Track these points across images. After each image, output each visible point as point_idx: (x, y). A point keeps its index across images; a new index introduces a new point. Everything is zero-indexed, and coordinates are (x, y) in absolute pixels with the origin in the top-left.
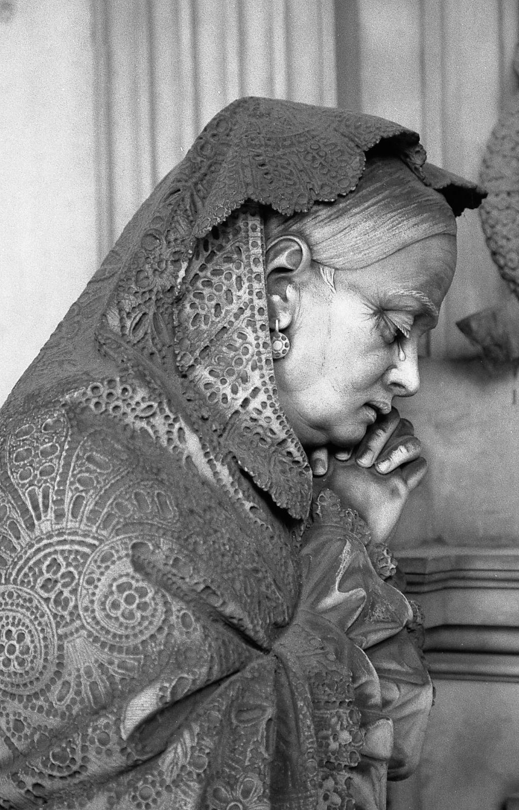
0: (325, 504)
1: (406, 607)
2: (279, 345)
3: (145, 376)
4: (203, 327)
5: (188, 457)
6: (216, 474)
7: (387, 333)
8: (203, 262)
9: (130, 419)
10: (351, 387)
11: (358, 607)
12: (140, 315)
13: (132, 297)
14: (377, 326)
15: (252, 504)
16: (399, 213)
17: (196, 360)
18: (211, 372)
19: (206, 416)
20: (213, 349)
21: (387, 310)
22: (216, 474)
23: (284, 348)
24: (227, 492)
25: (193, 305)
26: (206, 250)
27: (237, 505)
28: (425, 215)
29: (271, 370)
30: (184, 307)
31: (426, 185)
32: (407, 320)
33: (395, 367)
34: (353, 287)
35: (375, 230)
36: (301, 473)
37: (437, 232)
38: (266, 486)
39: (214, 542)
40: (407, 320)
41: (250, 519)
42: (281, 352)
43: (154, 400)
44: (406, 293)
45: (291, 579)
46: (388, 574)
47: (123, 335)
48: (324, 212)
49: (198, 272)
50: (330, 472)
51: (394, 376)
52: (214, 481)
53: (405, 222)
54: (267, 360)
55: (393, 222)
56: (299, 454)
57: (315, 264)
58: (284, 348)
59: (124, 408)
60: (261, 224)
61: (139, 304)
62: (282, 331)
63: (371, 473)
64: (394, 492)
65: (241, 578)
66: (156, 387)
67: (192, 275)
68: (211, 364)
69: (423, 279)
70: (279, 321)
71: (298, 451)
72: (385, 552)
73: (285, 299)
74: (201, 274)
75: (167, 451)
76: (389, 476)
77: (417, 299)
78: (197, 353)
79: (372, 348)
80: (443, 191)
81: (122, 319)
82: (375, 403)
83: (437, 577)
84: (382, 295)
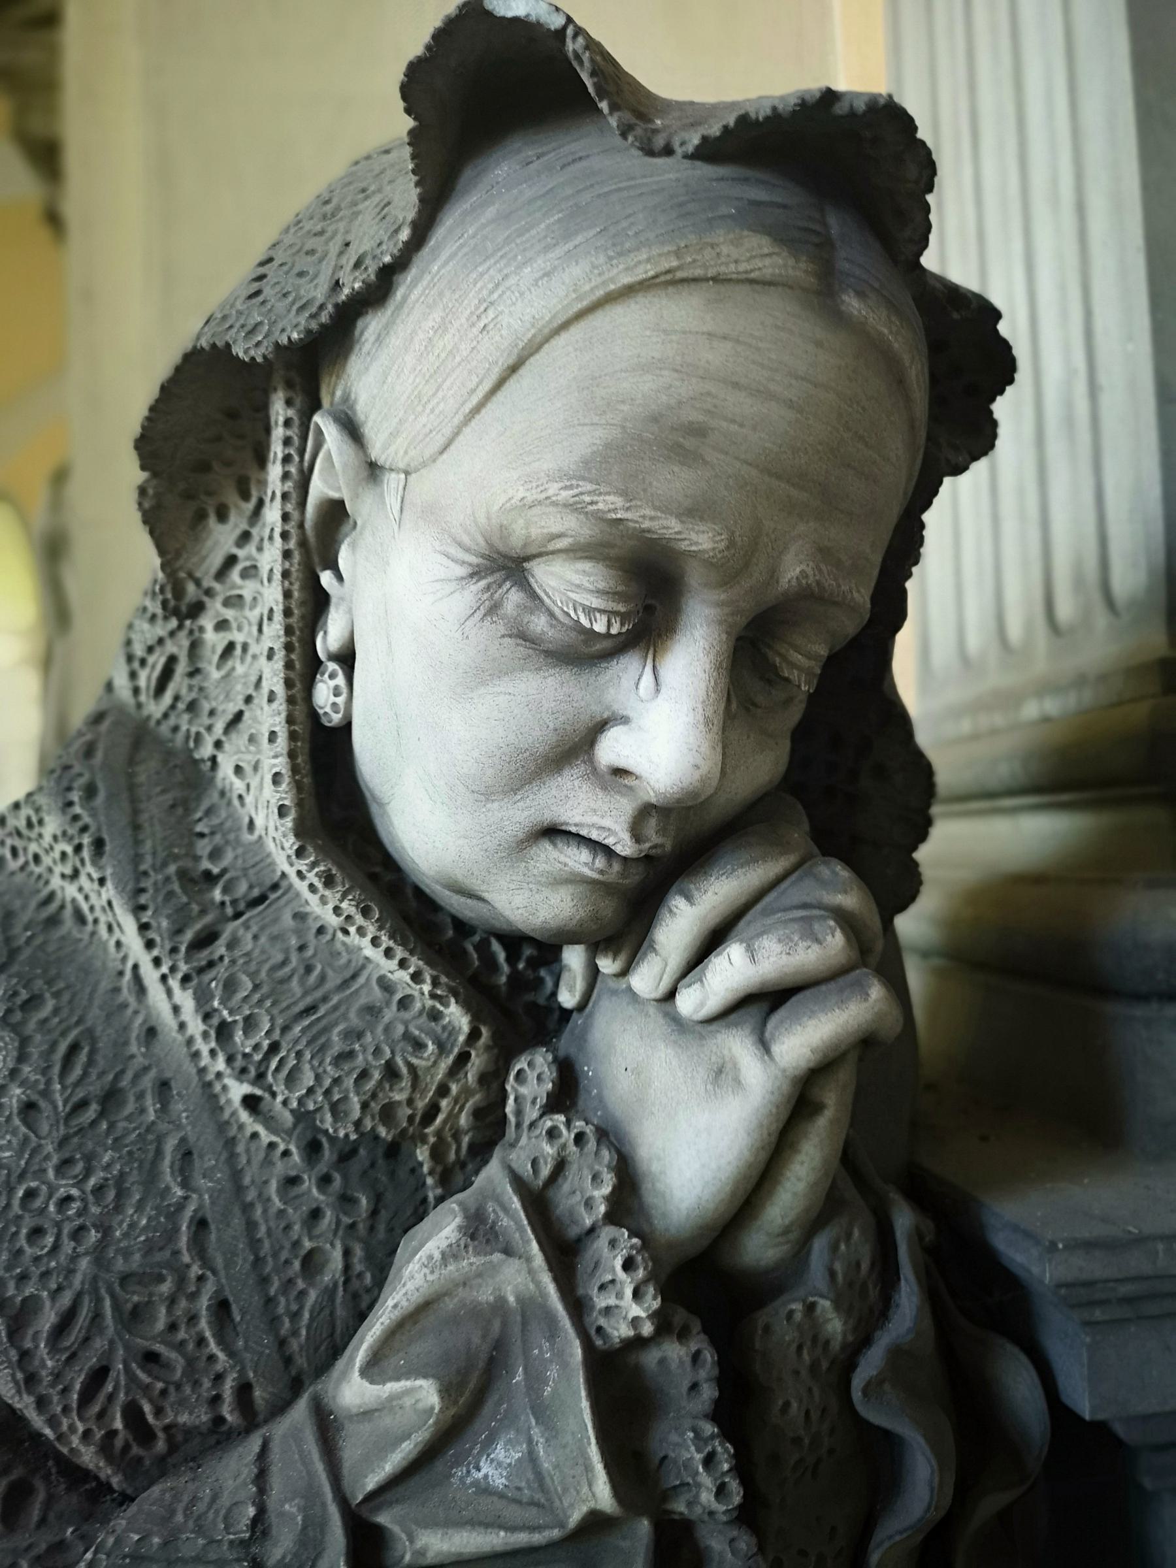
0: (523, 1090)
1: (588, 1468)
2: (324, 694)
3: (69, 789)
4: (240, 669)
5: (136, 967)
6: (176, 1009)
7: (539, 624)
8: (244, 526)
9: (56, 882)
10: (461, 788)
11: (407, 1436)
12: (162, 660)
13: (146, 626)
14: (494, 609)
15: (246, 1089)
16: (502, 257)
17: (218, 744)
18: (238, 770)
19: (216, 870)
20: (247, 715)
21: (528, 559)
22: (176, 1009)
23: (332, 699)
24: (196, 1055)
25: (222, 625)
26: (246, 496)
27: (217, 1088)
28: (579, 239)
29: (276, 757)
30: (201, 629)
31: (650, 152)
32: (576, 579)
33: (625, 720)
34: (431, 513)
35: (442, 328)
36: (435, 1016)
37: (627, 280)
38: (256, 1047)
39: (30, 1194)
40: (576, 579)
41: (241, 1127)
42: (328, 709)
43: (71, 839)
44: (531, 496)
45: (313, 1295)
46: (621, 1331)
47: (139, 706)
48: (371, 326)
49: (235, 551)
50: (590, 1004)
51: (613, 748)
52: (175, 1026)
53: (512, 281)
54: (272, 737)
55: (481, 289)
56: (393, 964)
57: (373, 470)
58: (332, 699)
59: (47, 860)
60: (289, 403)
61: (161, 641)
62: (334, 657)
63: (666, 1015)
64: (722, 1074)
65: (66, 1299)
66: (77, 809)
67: (217, 560)
68: (239, 752)
69: (589, 440)
70: (325, 633)
71: (388, 953)
72: (618, 1263)
73: (340, 578)
74: (241, 553)
75: (105, 950)
76: (713, 1027)
77: (573, 507)
78: (219, 727)
79: (486, 673)
80: (708, 152)
81: (133, 675)
82: (573, 829)
83: (1124, 1290)
84: (482, 520)
